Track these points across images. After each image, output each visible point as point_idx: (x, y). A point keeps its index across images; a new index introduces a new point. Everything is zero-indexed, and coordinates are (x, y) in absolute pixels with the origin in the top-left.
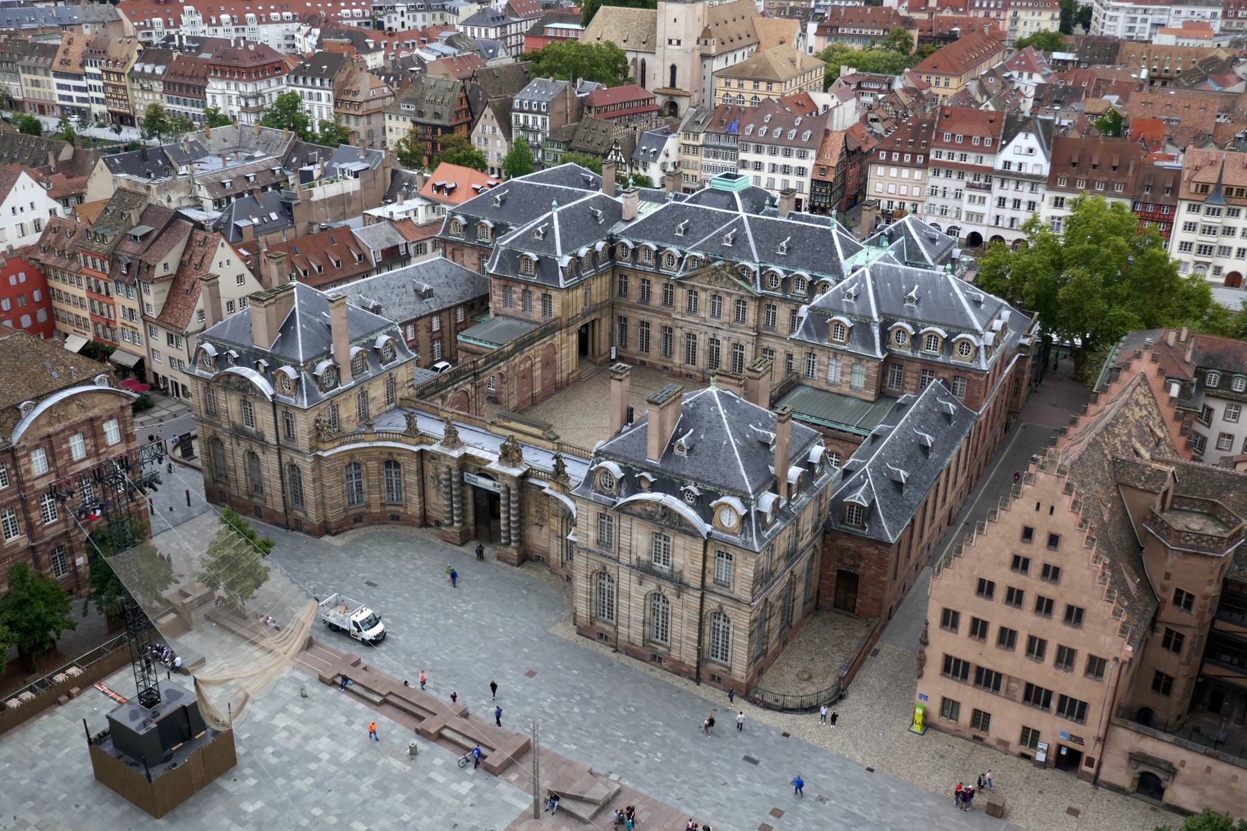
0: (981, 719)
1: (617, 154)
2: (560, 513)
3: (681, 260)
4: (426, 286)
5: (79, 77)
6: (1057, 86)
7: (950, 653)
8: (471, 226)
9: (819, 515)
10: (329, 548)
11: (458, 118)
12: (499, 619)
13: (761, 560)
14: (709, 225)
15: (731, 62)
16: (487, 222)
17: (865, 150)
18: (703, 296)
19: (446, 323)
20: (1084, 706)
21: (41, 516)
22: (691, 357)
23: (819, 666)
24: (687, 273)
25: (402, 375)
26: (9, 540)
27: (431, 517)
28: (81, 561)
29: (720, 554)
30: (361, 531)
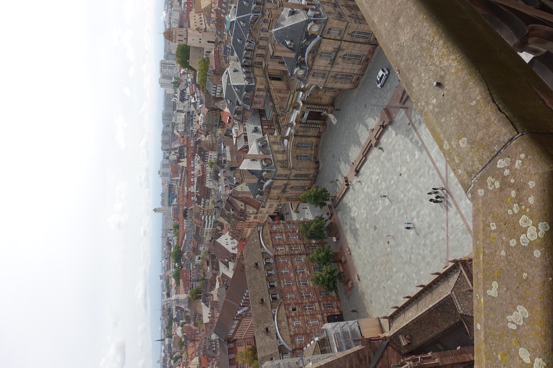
2: (317, 91)
3: (250, 42)
5: (205, 223)
11: (218, 114)
13: (332, 17)
18: (262, 35)
19: (266, 124)
26: (303, 260)
28: (314, 241)
29: (329, 33)
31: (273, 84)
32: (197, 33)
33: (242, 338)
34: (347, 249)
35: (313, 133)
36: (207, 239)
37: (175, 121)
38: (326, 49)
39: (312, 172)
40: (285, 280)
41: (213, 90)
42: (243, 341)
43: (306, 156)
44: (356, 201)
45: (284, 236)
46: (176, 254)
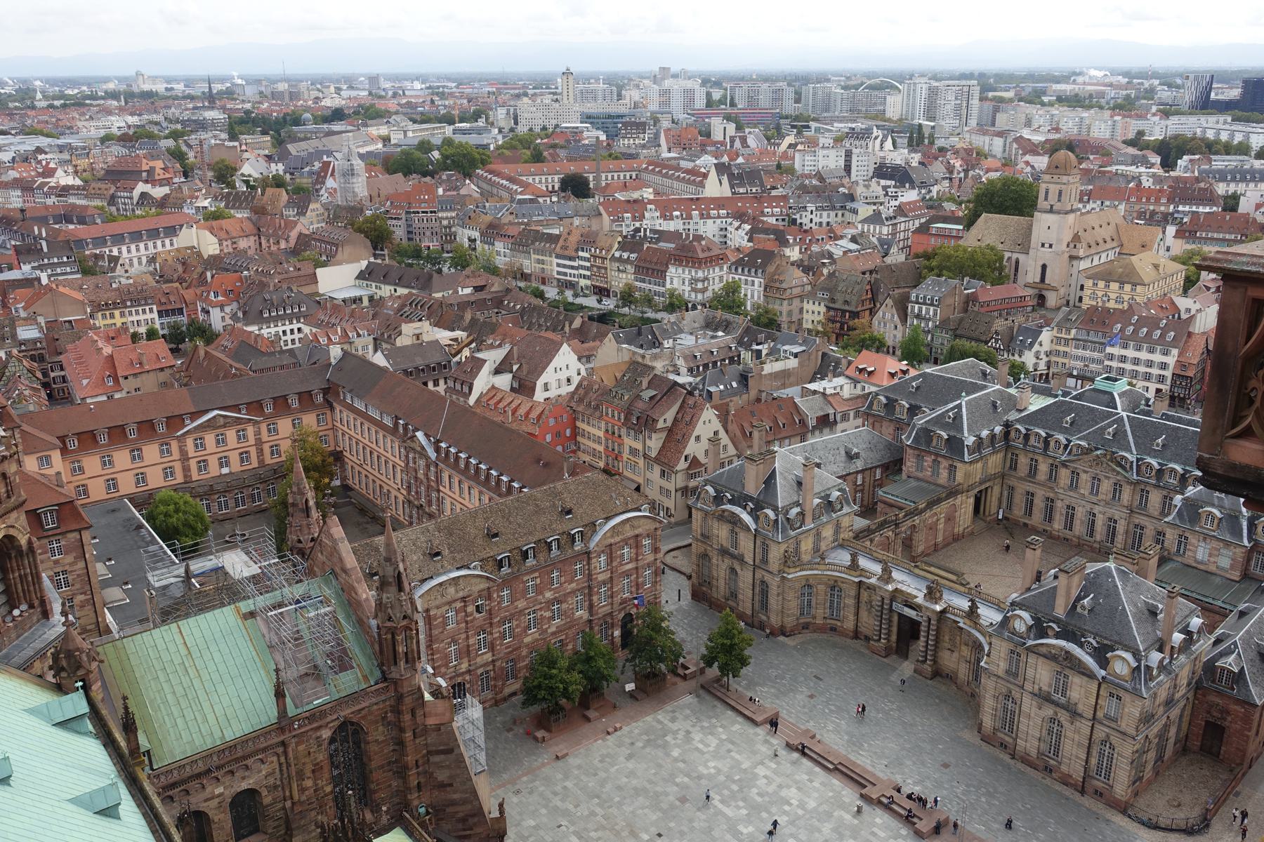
1: (997, 341)
2: (970, 643)
4: (855, 450)
8: (891, 405)
9: (1193, 673)
10: (784, 645)
12: (918, 719)
14: (1093, 420)
15: (1096, 262)
16: (904, 403)
18: (1083, 476)
19: (867, 480)
22: (1069, 523)
23: (1186, 798)
24: (1072, 458)
25: (845, 522)
28: (617, 633)
29: (1111, 695)
30: (807, 636)
32: (1068, 237)
33: (339, 425)
34: (618, 725)
36: (526, 262)
37: (821, 145)
39: (775, 620)
40: (538, 581)
41: (925, 297)
42: (331, 426)
43: (809, 605)
44: (730, 746)
46: (464, 156)
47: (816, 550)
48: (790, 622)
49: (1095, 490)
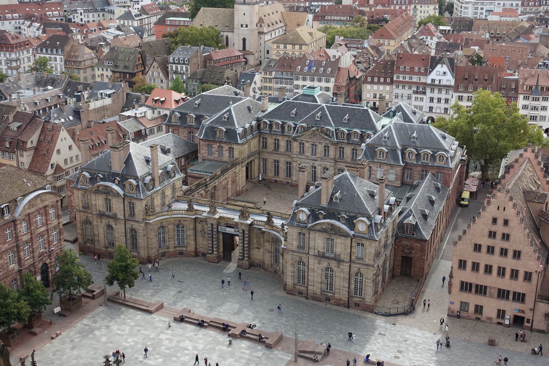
0: (479, 309)
2: (270, 240)
3: (295, 128)
4: (167, 147)
6: (446, 43)
7: (463, 280)
8: (183, 117)
9: (394, 230)
15: (273, 36)
16: (192, 115)
17: (357, 77)
18: (307, 145)
20: (524, 295)
21: (24, 254)
23: (400, 298)
24: (298, 134)
27: (200, 252)
28: (39, 278)
29: (358, 244)
30: (164, 261)
31: (242, 171)
32: (256, 20)
34: (58, 332)
35: (202, 245)
38: (337, 245)
39: (143, 253)
41: (179, 59)
43: (164, 241)
44: (139, 328)
45: (43, 229)
47: (163, 204)
48: (153, 253)
49: (314, 153)
